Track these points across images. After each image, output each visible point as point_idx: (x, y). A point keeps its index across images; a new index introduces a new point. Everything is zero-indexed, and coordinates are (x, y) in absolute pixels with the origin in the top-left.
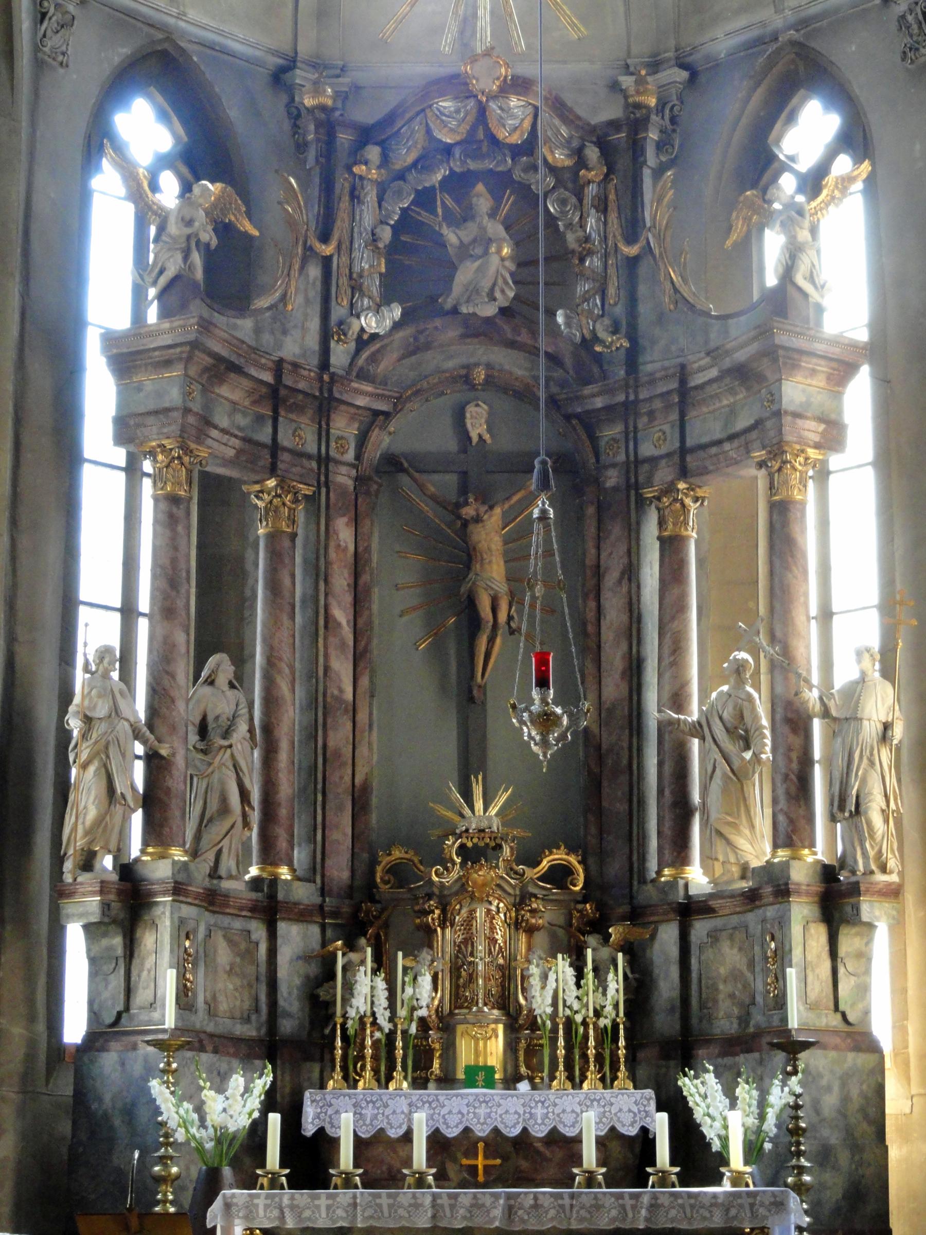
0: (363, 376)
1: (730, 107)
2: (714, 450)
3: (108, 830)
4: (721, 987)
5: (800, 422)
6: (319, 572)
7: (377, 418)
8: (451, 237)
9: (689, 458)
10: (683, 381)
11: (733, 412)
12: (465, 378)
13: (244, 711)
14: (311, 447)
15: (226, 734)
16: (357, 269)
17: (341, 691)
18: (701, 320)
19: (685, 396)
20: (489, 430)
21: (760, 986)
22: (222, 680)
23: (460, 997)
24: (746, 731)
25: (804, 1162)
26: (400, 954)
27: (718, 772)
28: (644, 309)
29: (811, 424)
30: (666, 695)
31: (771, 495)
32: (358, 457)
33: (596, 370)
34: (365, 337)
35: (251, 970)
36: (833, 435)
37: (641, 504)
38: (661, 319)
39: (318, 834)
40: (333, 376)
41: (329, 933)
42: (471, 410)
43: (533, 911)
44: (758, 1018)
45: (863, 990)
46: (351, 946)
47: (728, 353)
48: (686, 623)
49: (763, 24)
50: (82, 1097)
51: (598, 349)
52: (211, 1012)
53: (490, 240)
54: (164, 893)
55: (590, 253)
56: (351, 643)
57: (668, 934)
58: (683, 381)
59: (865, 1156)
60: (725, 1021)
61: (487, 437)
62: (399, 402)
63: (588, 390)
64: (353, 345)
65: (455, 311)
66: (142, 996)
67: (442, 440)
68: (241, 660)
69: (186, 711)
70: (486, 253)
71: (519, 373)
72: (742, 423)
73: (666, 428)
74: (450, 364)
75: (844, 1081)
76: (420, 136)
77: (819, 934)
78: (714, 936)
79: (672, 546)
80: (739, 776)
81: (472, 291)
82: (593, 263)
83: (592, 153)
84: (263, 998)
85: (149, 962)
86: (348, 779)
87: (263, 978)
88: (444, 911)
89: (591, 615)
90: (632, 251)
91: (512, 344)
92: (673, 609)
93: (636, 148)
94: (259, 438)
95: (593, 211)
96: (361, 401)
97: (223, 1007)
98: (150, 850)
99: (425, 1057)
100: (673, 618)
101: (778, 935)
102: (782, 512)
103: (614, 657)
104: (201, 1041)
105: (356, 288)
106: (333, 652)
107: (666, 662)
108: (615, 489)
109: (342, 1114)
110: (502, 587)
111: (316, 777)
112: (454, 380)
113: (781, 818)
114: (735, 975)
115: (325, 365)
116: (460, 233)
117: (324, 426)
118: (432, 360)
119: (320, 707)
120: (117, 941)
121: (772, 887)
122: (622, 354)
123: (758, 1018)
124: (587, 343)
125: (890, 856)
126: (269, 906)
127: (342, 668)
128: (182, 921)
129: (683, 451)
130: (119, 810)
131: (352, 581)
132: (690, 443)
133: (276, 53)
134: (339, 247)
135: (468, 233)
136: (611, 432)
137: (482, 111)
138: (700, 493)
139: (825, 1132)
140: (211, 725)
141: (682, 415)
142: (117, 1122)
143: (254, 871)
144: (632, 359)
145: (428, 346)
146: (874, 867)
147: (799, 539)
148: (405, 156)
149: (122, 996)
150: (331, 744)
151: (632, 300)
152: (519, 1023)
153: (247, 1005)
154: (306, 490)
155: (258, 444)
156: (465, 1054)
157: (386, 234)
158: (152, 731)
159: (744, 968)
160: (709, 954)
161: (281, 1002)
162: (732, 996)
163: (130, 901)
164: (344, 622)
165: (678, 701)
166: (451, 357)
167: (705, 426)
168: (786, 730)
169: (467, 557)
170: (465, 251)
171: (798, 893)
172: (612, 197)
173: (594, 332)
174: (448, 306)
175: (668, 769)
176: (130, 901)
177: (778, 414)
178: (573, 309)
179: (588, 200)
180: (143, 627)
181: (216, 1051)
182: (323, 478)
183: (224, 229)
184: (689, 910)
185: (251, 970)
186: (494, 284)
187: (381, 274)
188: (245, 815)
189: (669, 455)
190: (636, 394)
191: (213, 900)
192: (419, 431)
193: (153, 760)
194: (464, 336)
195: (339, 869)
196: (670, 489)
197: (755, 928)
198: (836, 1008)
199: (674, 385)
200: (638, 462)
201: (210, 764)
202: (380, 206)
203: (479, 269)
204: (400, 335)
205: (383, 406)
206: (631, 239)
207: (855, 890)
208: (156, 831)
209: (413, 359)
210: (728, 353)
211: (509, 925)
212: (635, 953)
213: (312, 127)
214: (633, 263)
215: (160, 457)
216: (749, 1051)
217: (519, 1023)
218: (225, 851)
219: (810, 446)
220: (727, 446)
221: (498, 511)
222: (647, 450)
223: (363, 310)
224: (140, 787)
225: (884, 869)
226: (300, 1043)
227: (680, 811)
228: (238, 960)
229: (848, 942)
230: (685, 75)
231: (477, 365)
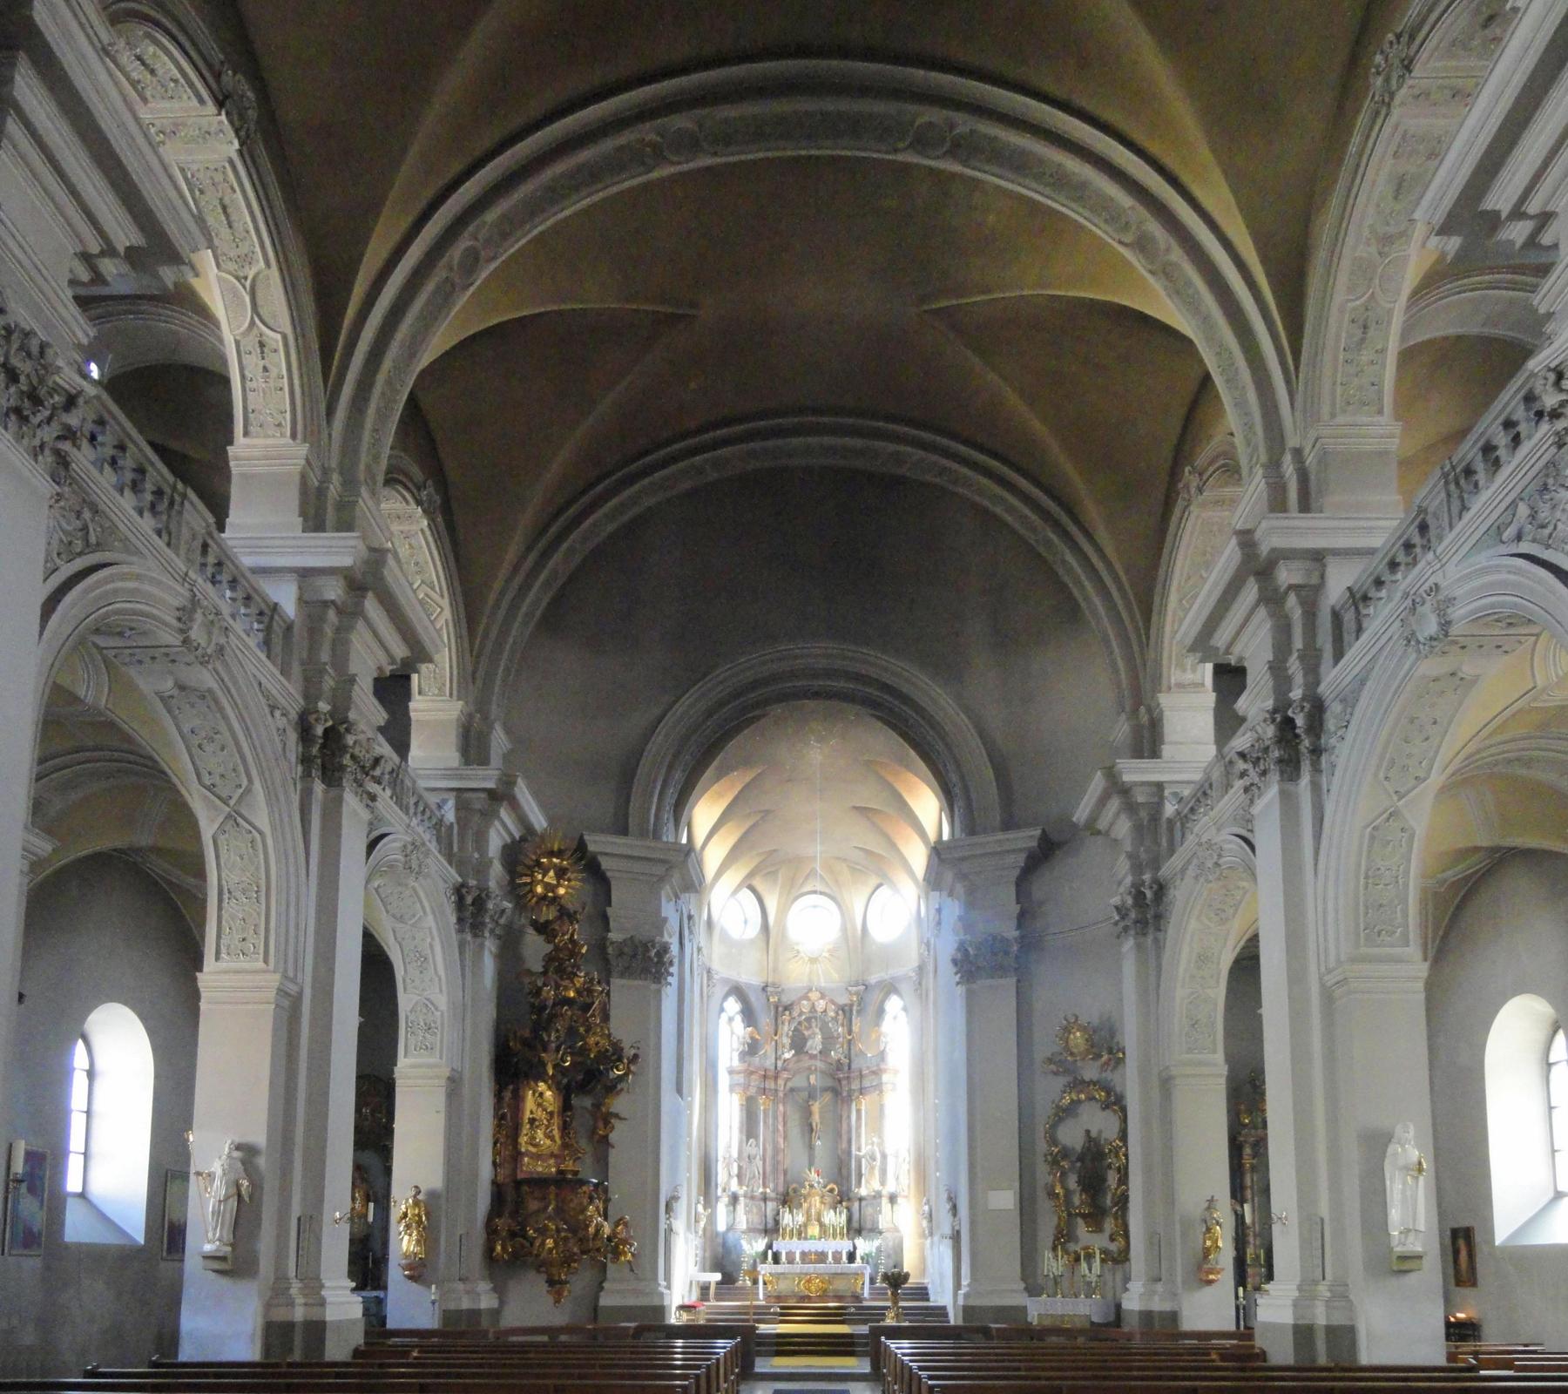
1: (875, 996)
3: (728, 1183)
6: (775, 1118)
7: (788, 1080)
23: (809, 1218)
39: (776, 1179)
50: (724, 1244)
57: (856, 1204)
60: (868, 1225)
67: (804, 1084)
68: (756, 1138)
79: (859, 1111)
80: (872, 1168)
92: (859, 1127)
94: (763, 1084)
99: (801, 1233)
102: (882, 1107)
103: (845, 1137)
109: (782, 1245)
111: (775, 1166)
119: (776, 1150)
121: (878, 1195)
126: (765, 1199)
127: (781, 1140)
148: (795, 1014)
152: (822, 1225)
156: (810, 1232)
163: (734, 1199)
165: (859, 1149)
167: (866, 1083)
183: (752, 1038)
184: (861, 1199)
191: (752, 1198)
192: (799, 1082)
193: (740, 1168)
195: (781, 1189)
208: (740, 1183)
212: (848, 1209)
217: (822, 1225)
226: (772, 1230)
227: (860, 1176)
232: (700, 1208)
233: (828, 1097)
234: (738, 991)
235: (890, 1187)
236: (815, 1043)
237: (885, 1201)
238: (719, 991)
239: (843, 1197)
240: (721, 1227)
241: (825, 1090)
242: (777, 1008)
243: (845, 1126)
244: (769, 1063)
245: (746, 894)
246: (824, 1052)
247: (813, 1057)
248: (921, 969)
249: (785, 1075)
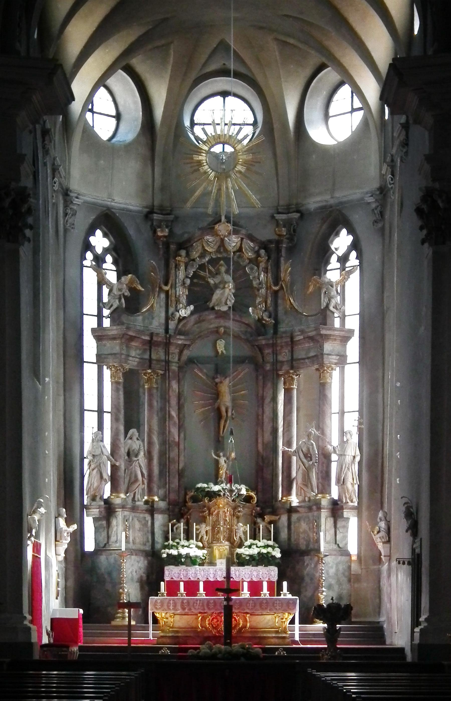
1: (314, 228)
2: (302, 361)
3: (100, 489)
4: (301, 535)
5: (330, 357)
8: (211, 281)
9: (294, 362)
11: (309, 349)
12: (217, 331)
13: (142, 448)
14: (163, 358)
15: (137, 456)
17: (174, 439)
18: (299, 315)
20: (225, 350)
21: (311, 536)
22: (135, 438)
24: (311, 455)
25: (324, 589)
26: (195, 524)
27: (301, 468)
28: (280, 308)
29: (334, 357)
30: (285, 441)
31: (320, 380)
32: (179, 360)
34: (181, 318)
35: (146, 529)
36: (342, 360)
37: (279, 376)
40: (170, 335)
41: (171, 517)
42: (219, 342)
43: (239, 512)
44: (311, 546)
45: (345, 537)
47: (306, 332)
49: (326, 201)
52: (134, 543)
53: (226, 283)
54: (119, 508)
55: (262, 288)
56: (177, 422)
57: (284, 519)
59: (343, 587)
61: (224, 352)
62: (193, 341)
63: (260, 338)
64: (176, 321)
66: (113, 539)
67: (209, 352)
68: (138, 426)
69: (123, 451)
70: (224, 288)
72: (312, 354)
74: (212, 326)
75: (337, 565)
76: (200, 248)
77: (331, 521)
78: (299, 520)
79: (288, 392)
82: (263, 291)
83: (262, 252)
84: (150, 537)
85: (115, 529)
86: (177, 467)
87: (150, 531)
88: (209, 511)
89: (260, 413)
90: (276, 288)
93: (278, 250)
95: (262, 273)
96: (180, 342)
97: (138, 541)
98: (114, 494)
101: (317, 521)
103: (268, 427)
104: (131, 552)
106: (171, 426)
107: (285, 430)
108: (268, 370)
110: (229, 404)
112: (212, 332)
113: (320, 485)
114: (305, 532)
115: (167, 330)
116: (215, 279)
117: (167, 350)
118: (205, 325)
120: (104, 522)
123: (311, 546)
124: (260, 320)
125: (354, 497)
127: (174, 431)
128: (125, 516)
129: (292, 359)
130: (103, 482)
131: (177, 401)
132: (295, 357)
133: (146, 207)
134: (171, 287)
135: (217, 280)
136: (267, 351)
137: (222, 240)
138: (298, 373)
139: (330, 580)
140: (131, 452)
141: (292, 348)
142: (106, 576)
143: (146, 498)
144: (276, 326)
145: (203, 321)
146: (348, 501)
147: (329, 396)
148: (195, 254)
149: (106, 539)
153: (145, 540)
154: (161, 372)
155: (146, 359)
157: (188, 281)
158: (113, 458)
159: (308, 530)
160: (297, 525)
161: (156, 539)
163: (109, 510)
164: (175, 416)
166: (211, 324)
167: (300, 353)
168: (322, 457)
169: (217, 395)
170: (216, 286)
171: (324, 509)
172: (269, 268)
173: (262, 316)
174: (211, 305)
176: (109, 510)
177: (322, 354)
178: (255, 307)
179: (261, 268)
180: (107, 418)
181: (136, 555)
182: (167, 368)
183: (132, 289)
184: (291, 510)
185: (146, 529)
186: (227, 300)
187: (186, 295)
188: (143, 481)
190: (276, 341)
191: (134, 509)
192: (201, 349)
193: (114, 467)
194: (216, 318)
196: (288, 372)
197: (311, 518)
198: (336, 543)
201: (131, 465)
202: (186, 271)
205: (188, 343)
206: (276, 284)
207: (342, 508)
208: (115, 489)
209: (199, 325)
210: (306, 332)
211: (231, 516)
213: (161, 244)
215: (113, 369)
216: (308, 555)
218: (137, 492)
219: (333, 364)
220: (307, 361)
222: (280, 358)
223: (180, 309)
224: (110, 475)
228: (142, 526)
229: (340, 524)
230: (299, 215)
232: (62, 522)
233: (246, 370)
234: (108, 220)
236: (225, 295)
237: (324, 514)
238: (82, 221)
239: (264, 505)
240: (89, 546)
241: (240, 361)
242: (167, 245)
244: (157, 324)
245: (121, 82)
246: (239, 307)
247: (223, 315)
248: (383, 191)
249: (180, 341)
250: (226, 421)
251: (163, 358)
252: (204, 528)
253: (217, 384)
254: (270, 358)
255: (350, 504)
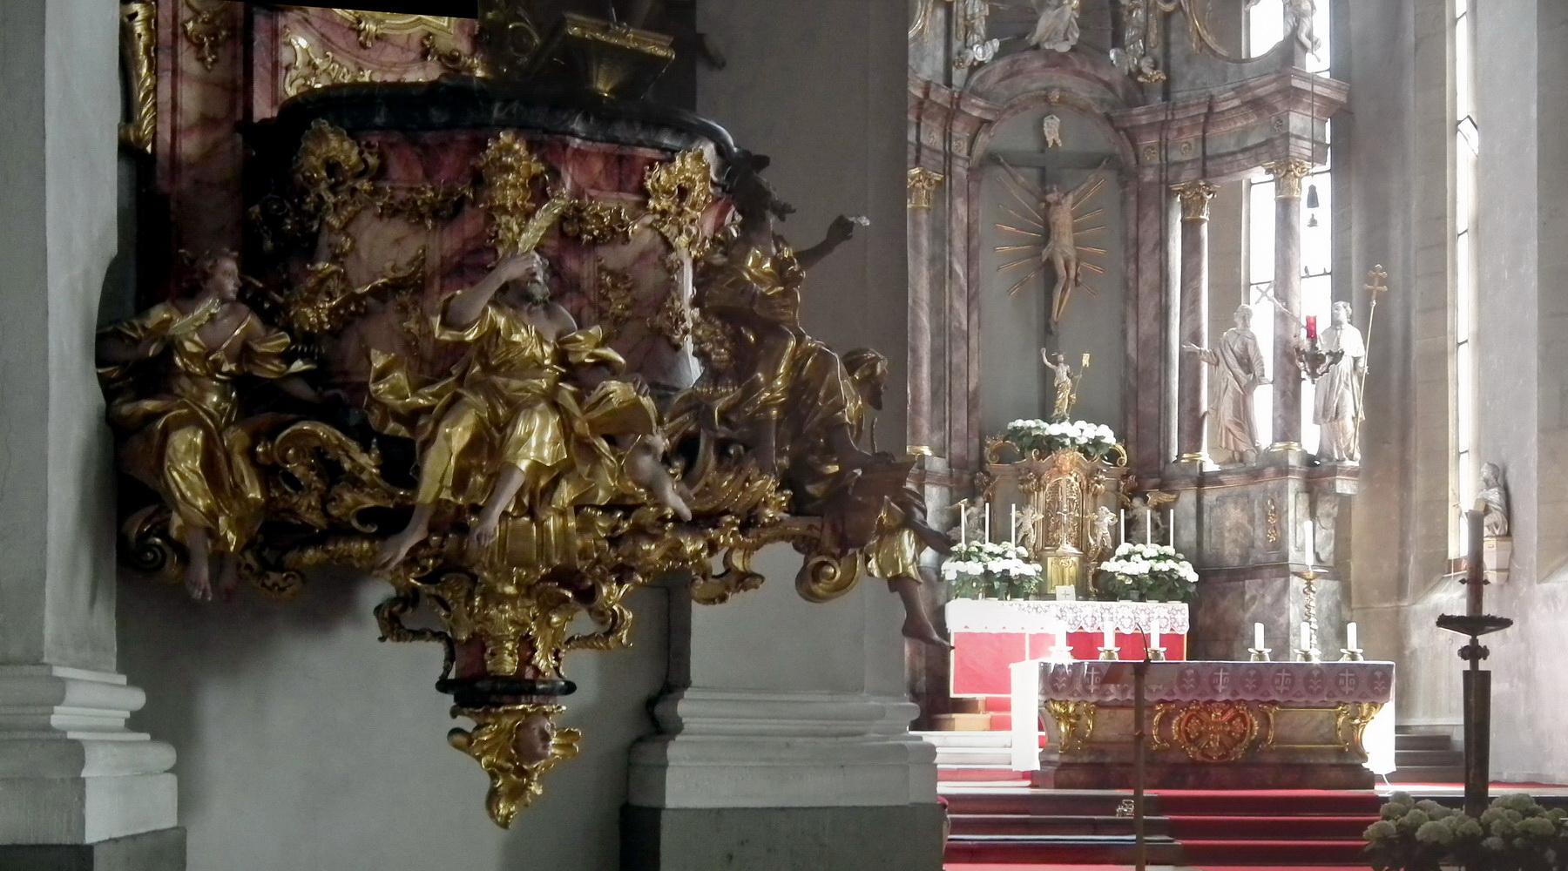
0: (975, 93)
10: (1210, 108)
14: (940, 146)
16: (969, 12)
19: (1211, 114)
28: (1175, 51)
30: (1187, 332)
32: (969, 154)
33: (1139, 96)
37: (1170, 194)
38: (1189, 59)
41: (955, 494)
42: (1047, 121)
44: (1258, 556)
46: (972, 503)
48: (1199, 282)
51: (1141, 79)
57: (1188, 498)
58: (1210, 108)
63: (1136, 111)
64: (966, 71)
65: (1037, 47)
67: (1028, 144)
71: (1083, 95)
73: (1191, 140)
74: (1034, 86)
77: (1303, 498)
78: (1222, 501)
81: (1052, 34)
89: (1131, 273)
91: (1080, 74)
96: (976, 113)
100: (1192, 279)
103: (1149, 308)
105: (969, 28)
106: (954, 295)
107: (1187, 310)
108: (1150, 183)
110: (1071, 253)
112: (1037, 98)
114: (1238, 527)
118: (1021, 82)
122: (1159, 85)
127: (960, 306)
129: (1205, 157)
141: (1204, 132)
145: (1019, 72)
150: (954, 361)
151: (1167, 45)
154: (938, 177)
160: (1217, 512)
162: (1235, 541)
166: (1033, 82)
167: (1223, 137)
169: (1047, 232)
174: (1034, 41)
175: (1187, 386)
189: (1193, 161)
192: (1010, 136)
199: (1205, 110)
200: (1169, 165)
203: (1057, 16)
204: (1000, 63)
205: (989, 117)
214: (1167, 16)
221: (1070, 197)
222: (1175, 156)
225: (1351, 458)
231: (1053, 87)
233: (1100, 184)
235: (1311, 438)
239: (1144, 475)
241: (1093, 162)
243: (1149, 275)
246: (1090, 49)
250: (1064, 290)
251: (940, 146)
252: (1032, 517)
253: (1048, 205)
254: (1153, 158)
255: (1348, 463)
